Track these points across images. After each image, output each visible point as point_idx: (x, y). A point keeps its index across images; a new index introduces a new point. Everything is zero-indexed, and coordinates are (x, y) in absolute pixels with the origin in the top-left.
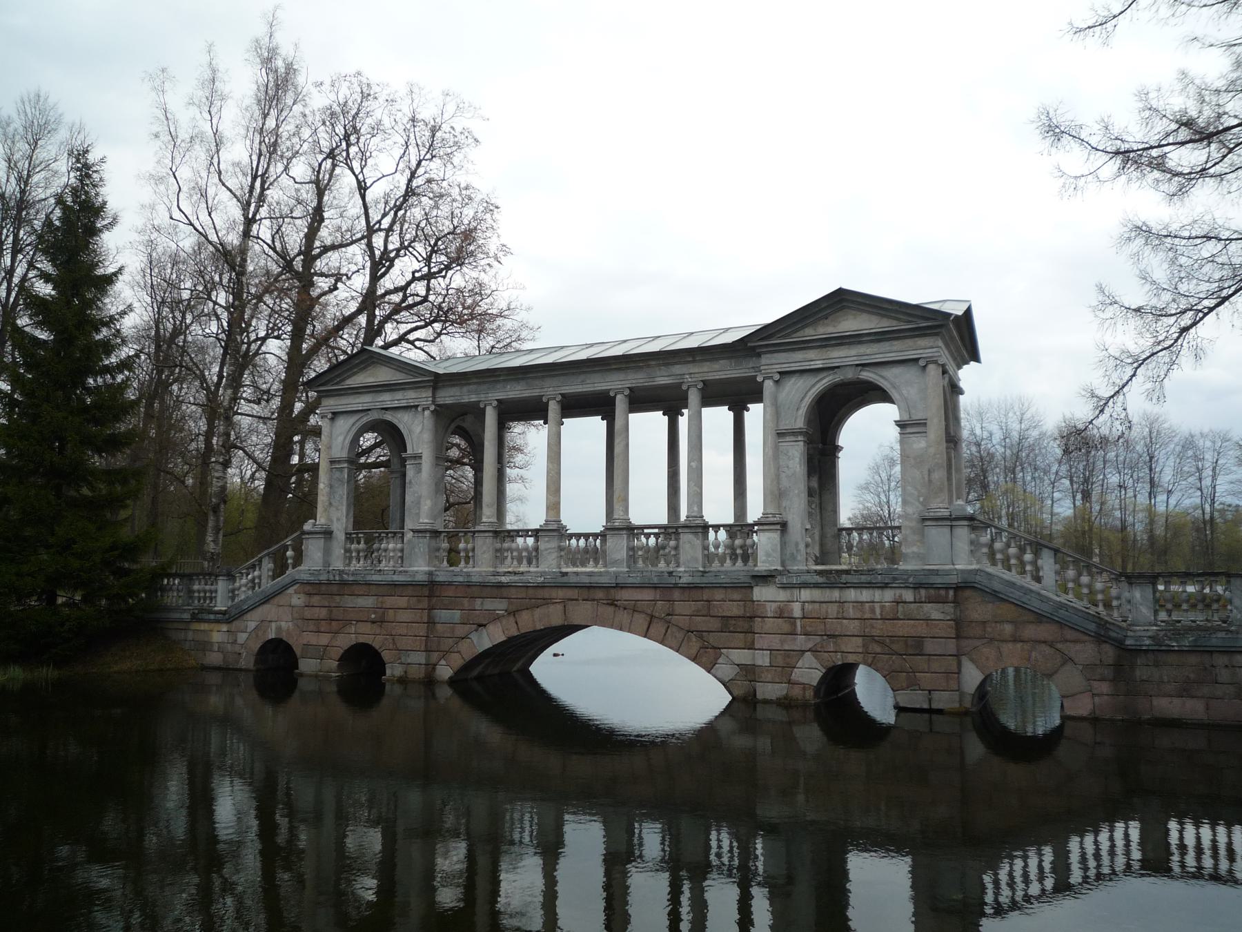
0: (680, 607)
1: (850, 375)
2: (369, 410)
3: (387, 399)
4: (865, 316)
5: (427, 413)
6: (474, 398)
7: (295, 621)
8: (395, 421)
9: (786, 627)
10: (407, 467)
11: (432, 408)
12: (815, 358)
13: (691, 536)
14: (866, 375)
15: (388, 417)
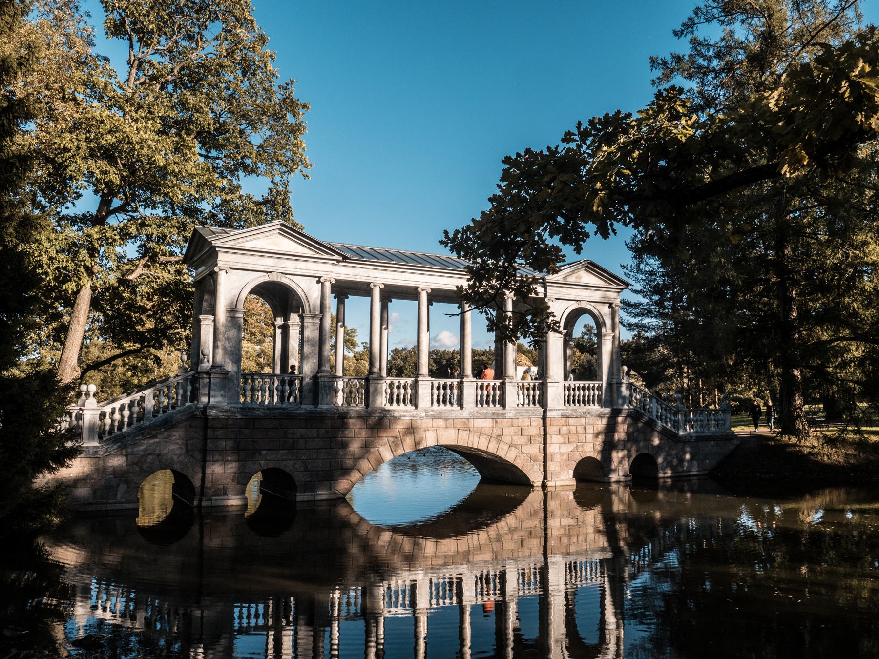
0: (506, 431)
1: (583, 305)
2: (270, 272)
3: (290, 266)
4: (592, 276)
5: (328, 285)
6: (365, 280)
7: (191, 453)
8: (293, 285)
9: (561, 440)
10: (305, 324)
11: (334, 282)
12: (573, 293)
13: (512, 388)
14: (589, 307)
15: (285, 280)
